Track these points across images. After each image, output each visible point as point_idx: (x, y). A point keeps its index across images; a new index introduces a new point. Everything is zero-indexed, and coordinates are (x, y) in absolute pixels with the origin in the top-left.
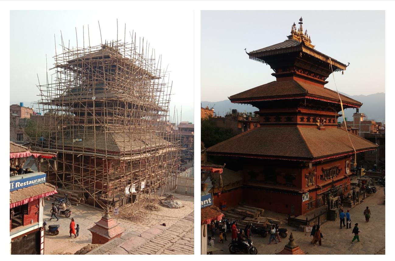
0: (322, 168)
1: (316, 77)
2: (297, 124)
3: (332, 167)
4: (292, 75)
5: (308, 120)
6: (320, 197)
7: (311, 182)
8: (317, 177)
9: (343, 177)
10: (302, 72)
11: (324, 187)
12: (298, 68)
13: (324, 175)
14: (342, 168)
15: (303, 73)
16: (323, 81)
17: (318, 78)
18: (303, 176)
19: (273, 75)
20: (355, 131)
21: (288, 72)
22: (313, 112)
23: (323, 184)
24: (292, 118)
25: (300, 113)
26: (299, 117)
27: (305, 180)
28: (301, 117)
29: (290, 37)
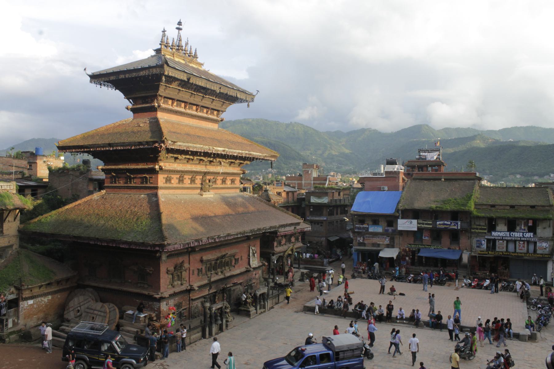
0: (202, 258)
1: (202, 111)
3: (219, 255)
4: (154, 110)
5: (181, 180)
6: (198, 303)
7: (179, 280)
8: (191, 272)
9: (243, 269)
10: (175, 104)
11: (200, 287)
14: (241, 257)
15: (177, 106)
16: (215, 118)
18: (163, 269)
20: (290, 194)
24: (152, 178)
26: (161, 179)
27: (165, 279)
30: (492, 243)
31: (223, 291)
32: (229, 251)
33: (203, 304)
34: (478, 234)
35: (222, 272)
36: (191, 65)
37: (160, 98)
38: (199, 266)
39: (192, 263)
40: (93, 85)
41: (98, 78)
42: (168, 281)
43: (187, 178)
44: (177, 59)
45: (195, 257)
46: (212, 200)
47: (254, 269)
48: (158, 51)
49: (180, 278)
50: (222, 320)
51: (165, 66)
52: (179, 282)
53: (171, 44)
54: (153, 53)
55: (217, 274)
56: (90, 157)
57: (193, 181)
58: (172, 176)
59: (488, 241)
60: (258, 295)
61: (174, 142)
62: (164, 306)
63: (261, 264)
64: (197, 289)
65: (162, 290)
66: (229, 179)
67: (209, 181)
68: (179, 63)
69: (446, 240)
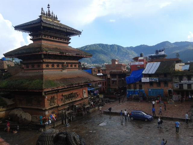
2: (43, 69)
4: (41, 39)
5: (53, 66)
8: (58, 100)
9: (80, 99)
10: (49, 37)
11: (62, 106)
12: (45, 35)
13: (63, 98)
16: (67, 42)
17: (63, 40)
18: (46, 100)
19: (31, 39)
20: (104, 71)
21: (38, 38)
22: (56, 61)
23: (62, 104)
25: (44, 62)
26: (44, 66)
28: (46, 64)
30: (181, 85)
31: (72, 106)
35: (71, 100)
36: (55, 21)
37: (42, 35)
39: (58, 96)
40: (16, 31)
41: (17, 28)
42: (48, 103)
44: (49, 19)
46: (66, 73)
47: (85, 98)
48: (40, 16)
49: (54, 102)
50: (70, 117)
51: (42, 22)
52: (53, 104)
53: (46, 14)
54: (39, 17)
55: (69, 100)
57: (58, 66)
58: (49, 64)
60: (86, 108)
61: (47, 51)
62: (47, 113)
63: (88, 96)
64: (60, 106)
65: (46, 106)
66: (73, 65)
67: (65, 66)
69: (162, 85)
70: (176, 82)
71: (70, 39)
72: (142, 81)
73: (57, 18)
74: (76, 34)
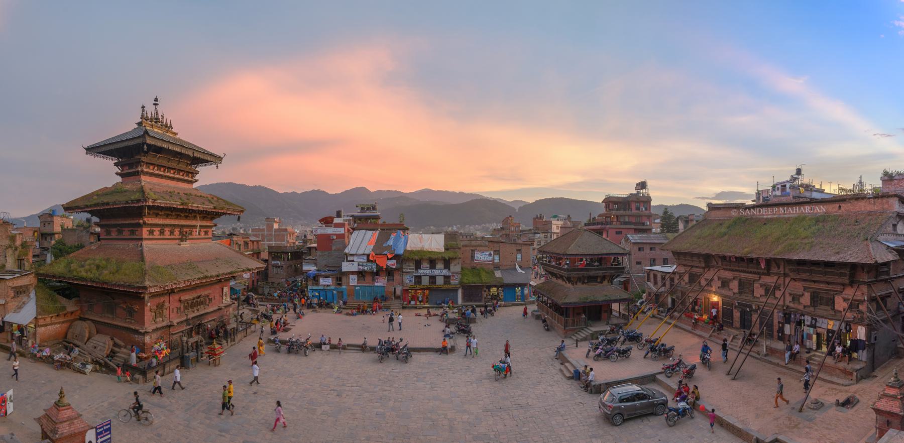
2: (141, 239)
3: (195, 295)
4: (137, 174)
5: (162, 233)
22: (168, 222)
26: (145, 231)
29: (140, 124)
32: (204, 292)
33: (181, 337)
34: (408, 273)
38: (178, 305)
39: (172, 303)
43: (167, 230)
45: (176, 297)
56: (89, 216)
57: (172, 233)
59: (416, 277)
68: (158, 133)
70: (408, 273)
71: (197, 172)
72: (343, 270)
73: (171, 127)
74: (208, 161)
